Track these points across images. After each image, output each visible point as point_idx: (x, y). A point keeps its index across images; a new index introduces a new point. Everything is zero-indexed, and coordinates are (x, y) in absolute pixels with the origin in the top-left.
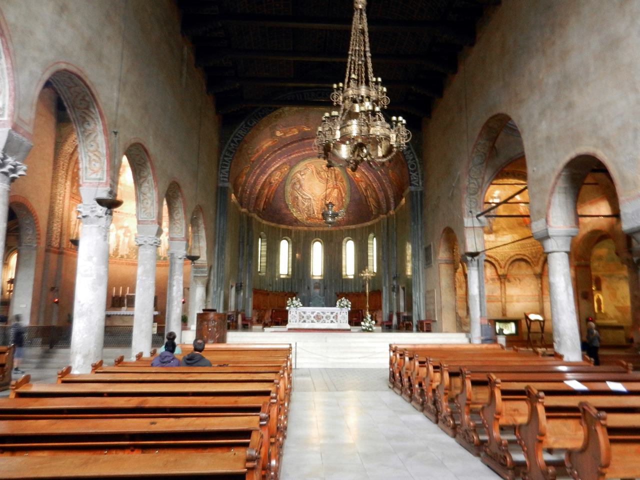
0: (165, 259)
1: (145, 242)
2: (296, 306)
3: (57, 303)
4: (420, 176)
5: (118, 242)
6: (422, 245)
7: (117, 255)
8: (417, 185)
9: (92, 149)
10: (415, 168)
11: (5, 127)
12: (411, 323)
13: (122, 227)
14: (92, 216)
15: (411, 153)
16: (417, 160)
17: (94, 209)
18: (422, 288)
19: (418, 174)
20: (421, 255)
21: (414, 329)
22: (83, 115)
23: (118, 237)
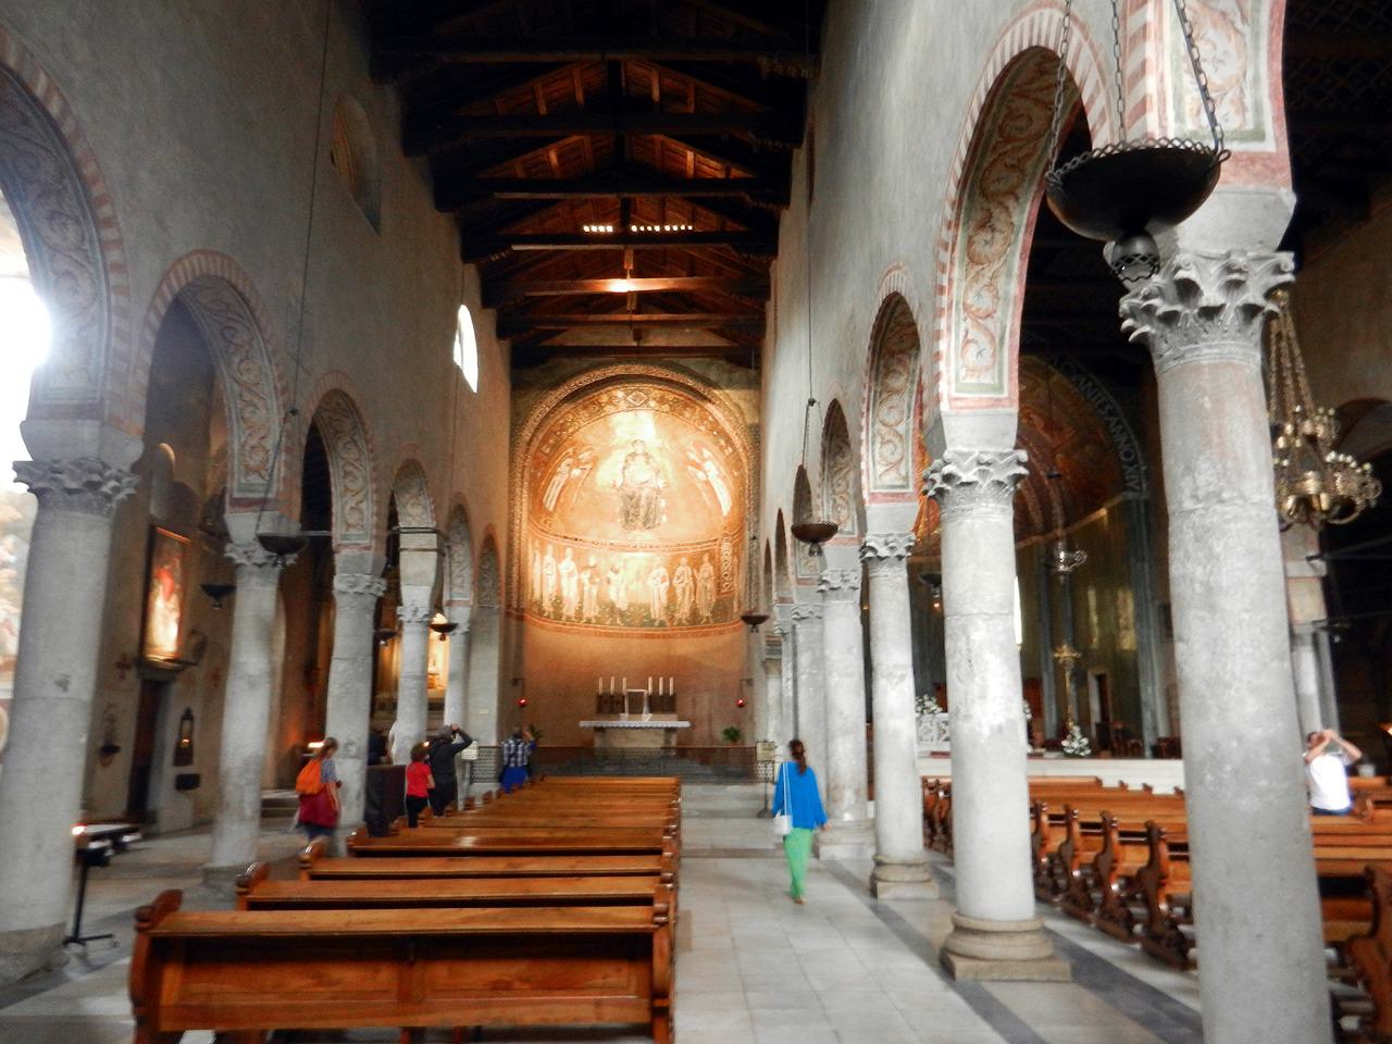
0: (662, 624)
1: (811, 612)
2: (933, 712)
3: (523, 705)
4: (1142, 472)
5: (582, 593)
6: (1153, 600)
7: (581, 619)
8: (1138, 488)
9: (837, 490)
10: (1132, 458)
11: (911, 501)
12: (1140, 742)
13: (588, 567)
14: (845, 587)
15: (1123, 430)
16: (1136, 443)
17: (846, 578)
18: (1157, 679)
19: (1138, 469)
20: (1151, 619)
21: (1148, 753)
22: (842, 444)
23: (580, 584)
